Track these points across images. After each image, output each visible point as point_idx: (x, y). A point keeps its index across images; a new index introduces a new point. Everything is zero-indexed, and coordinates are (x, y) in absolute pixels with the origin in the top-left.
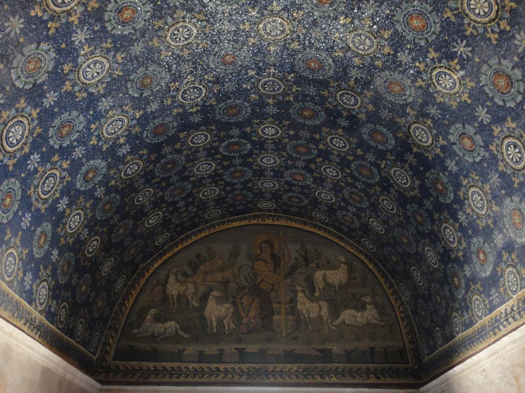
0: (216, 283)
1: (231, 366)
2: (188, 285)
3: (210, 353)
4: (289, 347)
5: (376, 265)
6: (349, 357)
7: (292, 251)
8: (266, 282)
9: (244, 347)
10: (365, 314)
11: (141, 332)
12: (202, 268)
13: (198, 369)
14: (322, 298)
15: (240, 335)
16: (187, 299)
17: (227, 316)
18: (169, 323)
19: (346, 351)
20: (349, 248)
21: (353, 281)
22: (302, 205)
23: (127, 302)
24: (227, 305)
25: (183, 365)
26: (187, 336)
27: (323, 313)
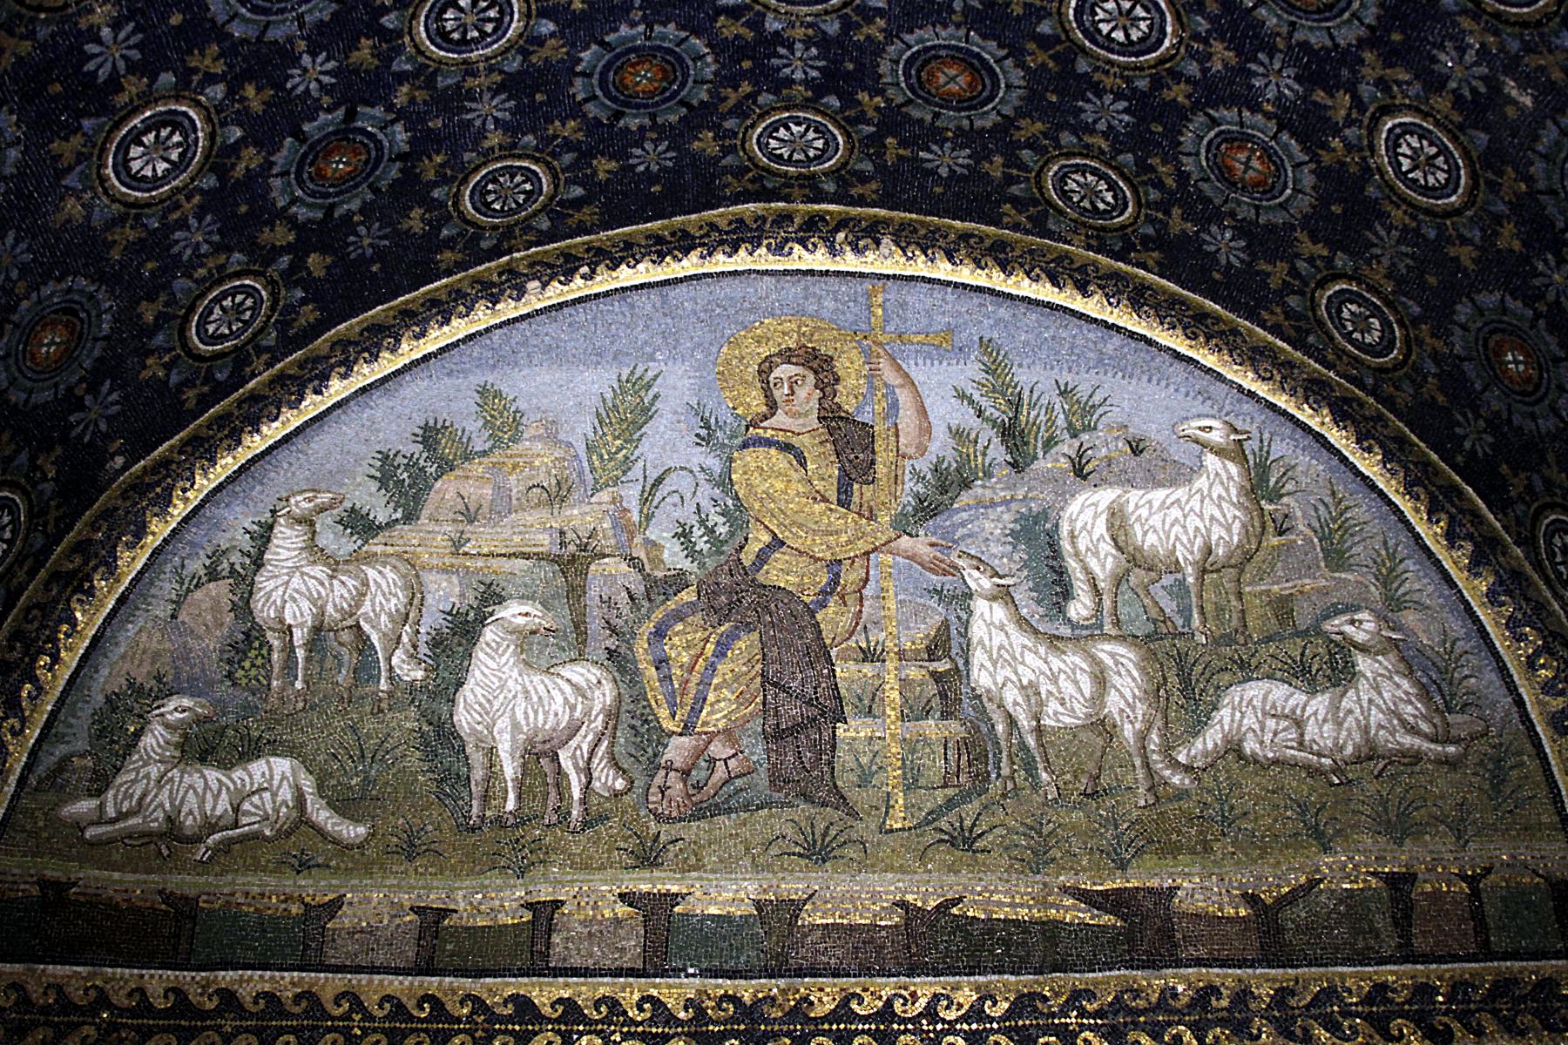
0: (521, 563)
1: (605, 987)
2: (371, 573)
3: (481, 922)
4: (925, 893)
5: (1395, 451)
6: (1269, 932)
7: (935, 404)
9: (674, 889)
10: (1346, 704)
11: (111, 811)
12: (446, 490)
13: (411, 1005)
14: (1108, 628)
15: (653, 827)
16: (362, 643)
17: (574, 729)
18: (258, 768)
19: (1252, 900)
20: (1248, 381)
21: (1275, 541)
22: (987, 119)
23: (45, 660)
24: (581, 673)
25: (328, 984)
26: (354, 831)
27: (1113, 703)
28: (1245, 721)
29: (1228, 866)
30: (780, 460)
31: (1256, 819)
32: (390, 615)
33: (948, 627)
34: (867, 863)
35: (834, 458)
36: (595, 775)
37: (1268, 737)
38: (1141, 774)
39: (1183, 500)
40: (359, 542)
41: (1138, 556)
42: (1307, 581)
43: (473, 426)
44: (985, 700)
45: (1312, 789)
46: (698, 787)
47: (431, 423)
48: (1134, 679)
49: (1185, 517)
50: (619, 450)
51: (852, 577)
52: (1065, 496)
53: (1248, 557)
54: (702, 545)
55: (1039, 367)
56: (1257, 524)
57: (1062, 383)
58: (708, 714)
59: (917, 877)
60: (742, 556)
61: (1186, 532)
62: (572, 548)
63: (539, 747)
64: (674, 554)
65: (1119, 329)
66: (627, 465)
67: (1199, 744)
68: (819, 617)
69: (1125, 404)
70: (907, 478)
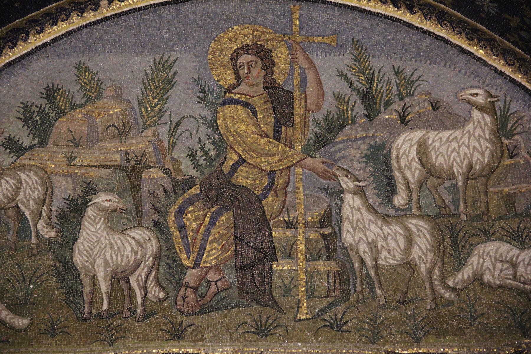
0: (105, 171)
2: (23, 176)
8: (254, 167)
12: (62, 126)
14: (415, 211)
16: (20, 216)
17: (137, 265)
20: (499, 65)
21: (508, 162)
24: (138, 234)
26: (22, 322)
27: (416, 252)
28: (485, 264)
29: (473, 342)
30: (241, 112)
31: (489, 317)
32: (35, 200)
33: (330, 210)
34: (288, 336)
35: (271, 111)
36: (149, 290)
37: (497, 273)
38: (428, 291)
39: (459, 137)
40: (15, 158)
41: (433, 170)
42: (524, 185)
43: (75, 89)
44: (349, 250)
45: (519, 302)
46: (202, 297)
47: (50, 86)
48: (427, 240)
49: (459, 147)
50: (156, 105)
51: (281, 181)
52: (394, 135)
53: (492, 171)
54: (202, 162)
55: (383, 58)
56: (499, 151)
57: (396, 66)
58: (207, 257)
59: (313, 345)
60: (223, 168)
61: (459, 156)
62: (133, 163)
63: (119, 275)
64: (188, 167)
65: (429, 33)
66: (161, 113)
67: (460, 276)
68: (264, 203)
69: (431, 80)
70: (311, 123)
